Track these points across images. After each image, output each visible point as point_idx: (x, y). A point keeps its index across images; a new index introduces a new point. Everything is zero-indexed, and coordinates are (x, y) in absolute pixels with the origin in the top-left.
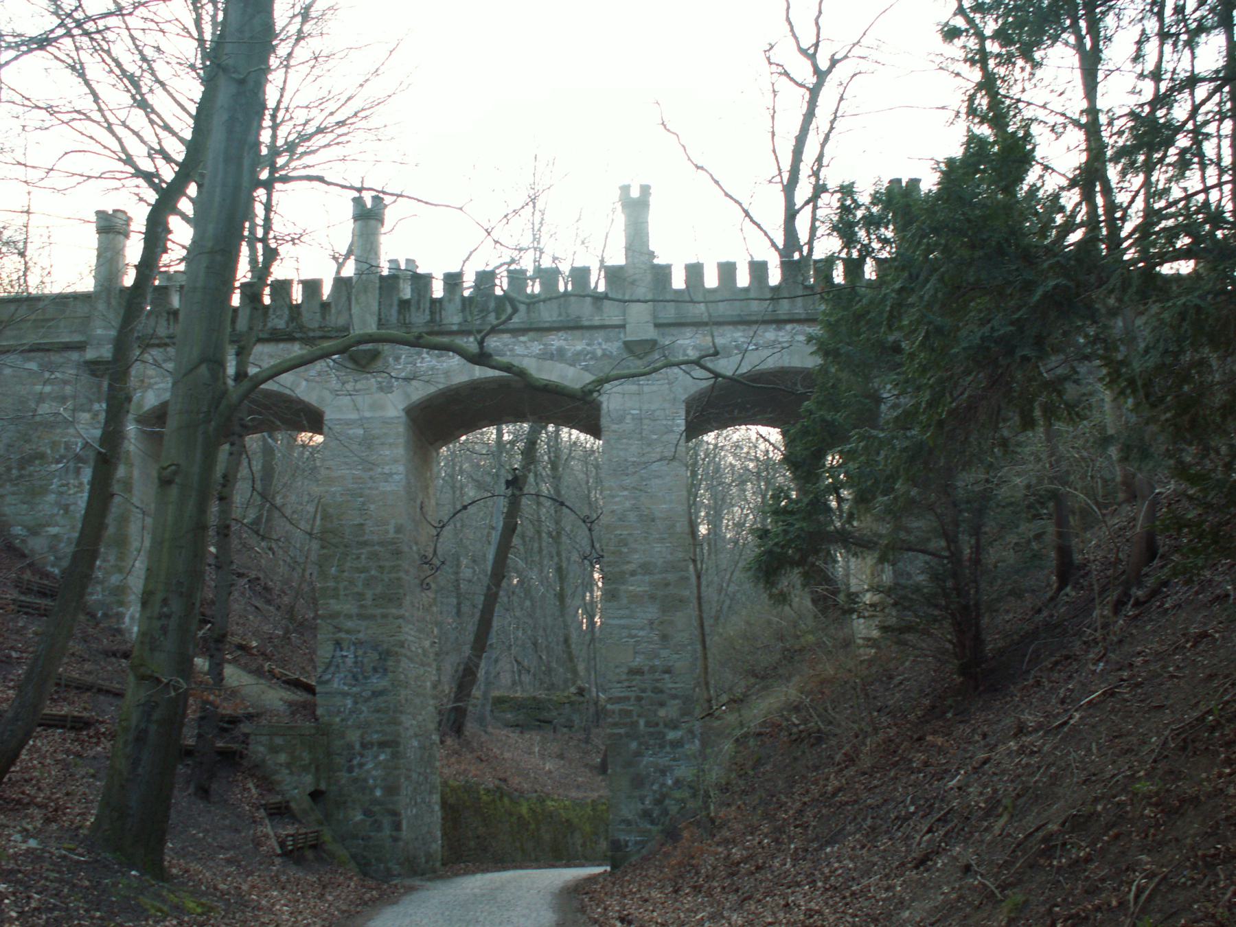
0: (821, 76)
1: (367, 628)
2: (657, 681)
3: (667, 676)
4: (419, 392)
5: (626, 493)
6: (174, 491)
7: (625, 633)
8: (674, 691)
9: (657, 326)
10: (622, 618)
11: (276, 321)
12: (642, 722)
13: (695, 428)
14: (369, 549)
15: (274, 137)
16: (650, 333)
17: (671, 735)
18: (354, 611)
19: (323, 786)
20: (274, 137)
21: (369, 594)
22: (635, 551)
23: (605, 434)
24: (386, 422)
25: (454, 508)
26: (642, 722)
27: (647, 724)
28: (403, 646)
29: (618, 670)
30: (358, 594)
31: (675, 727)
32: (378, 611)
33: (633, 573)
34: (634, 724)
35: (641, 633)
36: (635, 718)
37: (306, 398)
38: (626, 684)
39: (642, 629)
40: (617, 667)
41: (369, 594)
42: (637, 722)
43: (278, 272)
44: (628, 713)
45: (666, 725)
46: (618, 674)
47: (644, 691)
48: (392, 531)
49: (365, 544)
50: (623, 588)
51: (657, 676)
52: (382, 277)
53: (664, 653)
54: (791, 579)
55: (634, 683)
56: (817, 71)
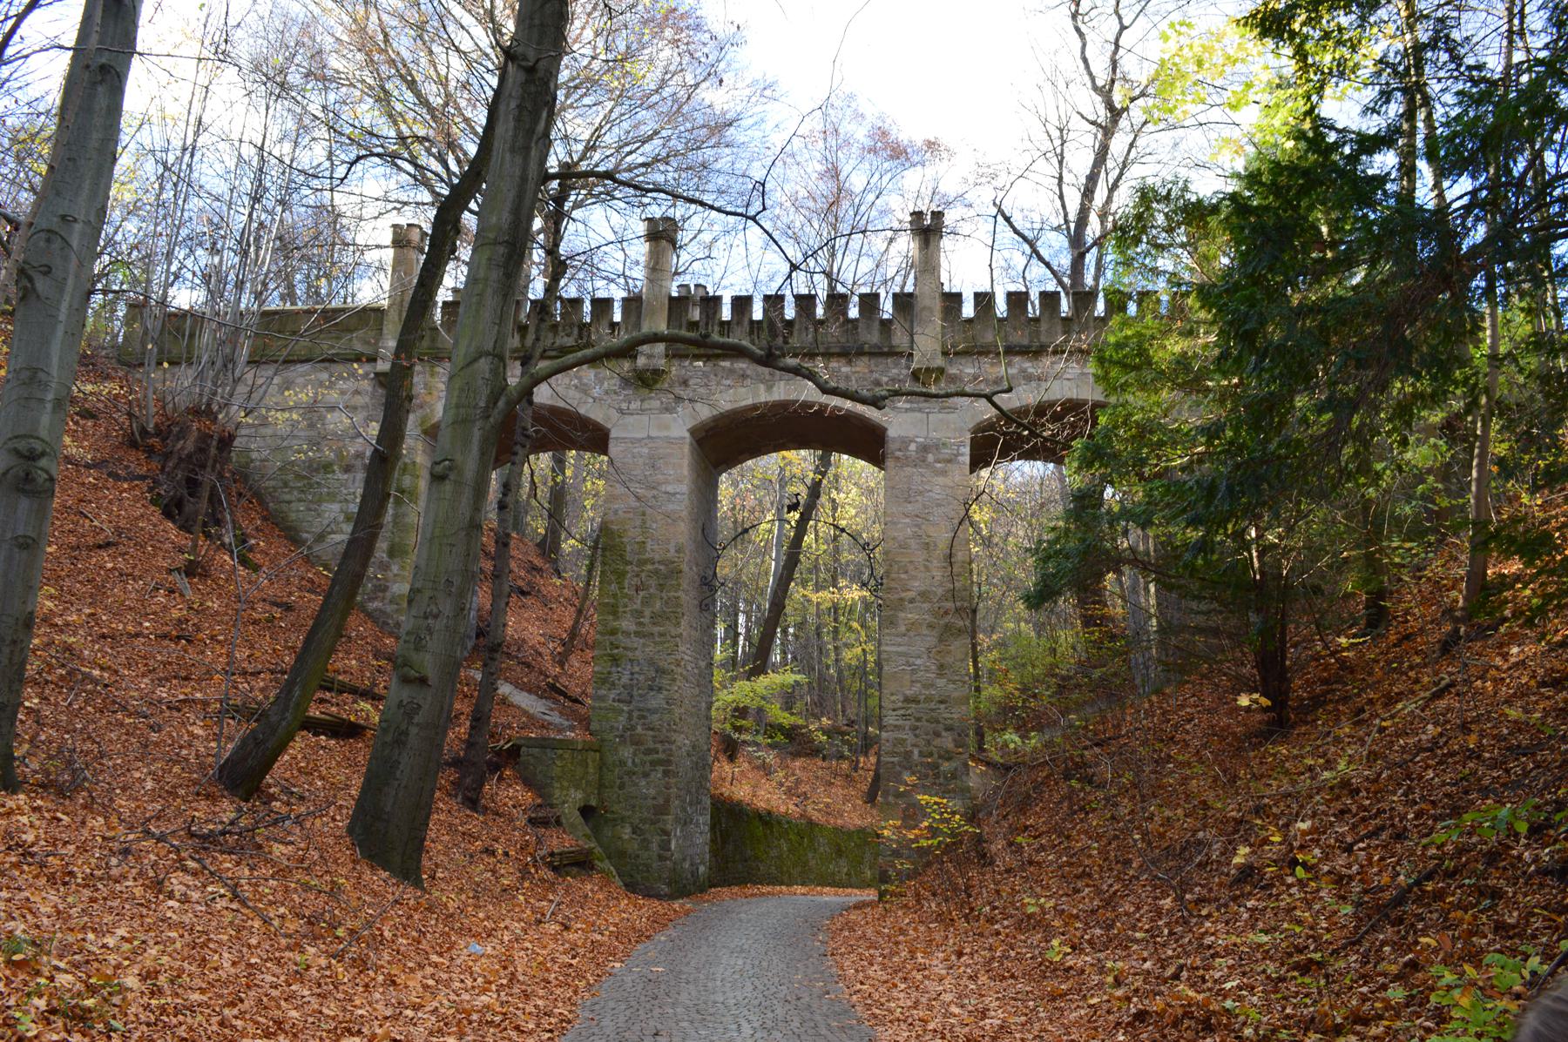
0: (1116, 113)
1: (644, 645)
2: (932, 710)
3: (942, 706)
4: (705, 413)
5: (907, 520)
6: (448, 487)
7: (902, 660)
8: (949, 722)
9: (945, 353)
10: (900, 645)
11: (566, 339)
12: (916, 752)
13: (980, 459)
14: (650, 567)
15: (1109, 199)
16: (939, 361)
17: (946, 766)
18: (633, 628)
19: (593, 803)
20: (1109, 199)
21: (647, 613)
22: (914, 578)
23: (889, 463)
24: (670, 441)
25: (736, 530)
26: (916, 752)
27: (921, 754)
28: (678, 665)
29: (893, 698)
30: (636, 611)
31: (949, 759)
32: (656, 629)
33: (912, 601)
34: (908, 755)
35: (918, 662)
36: (909, 748)
37: (592, 416)
38: (902, 712)
39: (919, 657)
40: (892, 694)
41: (647, 613)
42: (912, 752)
43: (569, 290)
44: (902, 742)
45: (940, 757)
46: (894, 702)
47: (919, 720)
48: (672, 551)
49: (645, 562)
50: (902, 615)
51: (932, 705)
52: (671, 299)
53: (941, 682)
54: (1066, 603)
55: (909, 712)
56: (1110, 106)
